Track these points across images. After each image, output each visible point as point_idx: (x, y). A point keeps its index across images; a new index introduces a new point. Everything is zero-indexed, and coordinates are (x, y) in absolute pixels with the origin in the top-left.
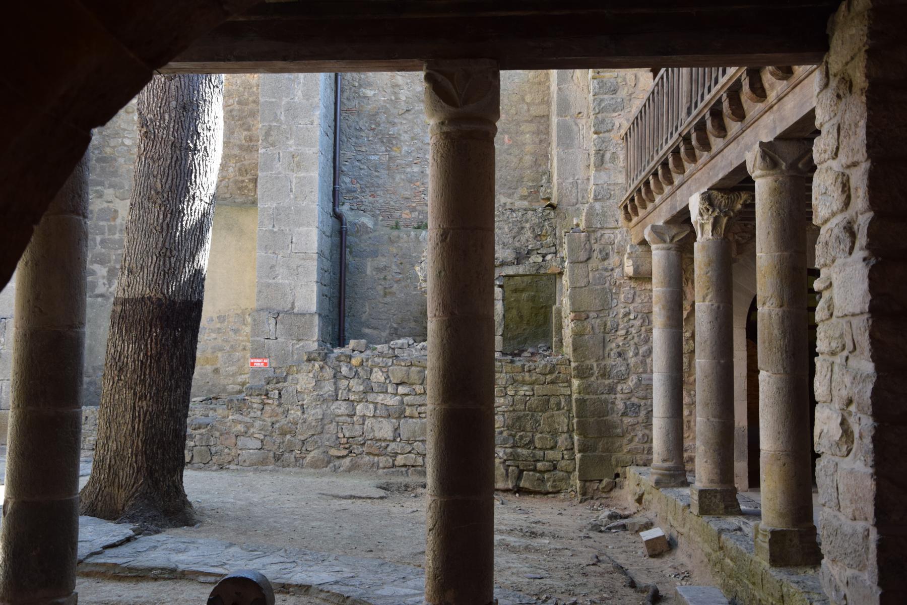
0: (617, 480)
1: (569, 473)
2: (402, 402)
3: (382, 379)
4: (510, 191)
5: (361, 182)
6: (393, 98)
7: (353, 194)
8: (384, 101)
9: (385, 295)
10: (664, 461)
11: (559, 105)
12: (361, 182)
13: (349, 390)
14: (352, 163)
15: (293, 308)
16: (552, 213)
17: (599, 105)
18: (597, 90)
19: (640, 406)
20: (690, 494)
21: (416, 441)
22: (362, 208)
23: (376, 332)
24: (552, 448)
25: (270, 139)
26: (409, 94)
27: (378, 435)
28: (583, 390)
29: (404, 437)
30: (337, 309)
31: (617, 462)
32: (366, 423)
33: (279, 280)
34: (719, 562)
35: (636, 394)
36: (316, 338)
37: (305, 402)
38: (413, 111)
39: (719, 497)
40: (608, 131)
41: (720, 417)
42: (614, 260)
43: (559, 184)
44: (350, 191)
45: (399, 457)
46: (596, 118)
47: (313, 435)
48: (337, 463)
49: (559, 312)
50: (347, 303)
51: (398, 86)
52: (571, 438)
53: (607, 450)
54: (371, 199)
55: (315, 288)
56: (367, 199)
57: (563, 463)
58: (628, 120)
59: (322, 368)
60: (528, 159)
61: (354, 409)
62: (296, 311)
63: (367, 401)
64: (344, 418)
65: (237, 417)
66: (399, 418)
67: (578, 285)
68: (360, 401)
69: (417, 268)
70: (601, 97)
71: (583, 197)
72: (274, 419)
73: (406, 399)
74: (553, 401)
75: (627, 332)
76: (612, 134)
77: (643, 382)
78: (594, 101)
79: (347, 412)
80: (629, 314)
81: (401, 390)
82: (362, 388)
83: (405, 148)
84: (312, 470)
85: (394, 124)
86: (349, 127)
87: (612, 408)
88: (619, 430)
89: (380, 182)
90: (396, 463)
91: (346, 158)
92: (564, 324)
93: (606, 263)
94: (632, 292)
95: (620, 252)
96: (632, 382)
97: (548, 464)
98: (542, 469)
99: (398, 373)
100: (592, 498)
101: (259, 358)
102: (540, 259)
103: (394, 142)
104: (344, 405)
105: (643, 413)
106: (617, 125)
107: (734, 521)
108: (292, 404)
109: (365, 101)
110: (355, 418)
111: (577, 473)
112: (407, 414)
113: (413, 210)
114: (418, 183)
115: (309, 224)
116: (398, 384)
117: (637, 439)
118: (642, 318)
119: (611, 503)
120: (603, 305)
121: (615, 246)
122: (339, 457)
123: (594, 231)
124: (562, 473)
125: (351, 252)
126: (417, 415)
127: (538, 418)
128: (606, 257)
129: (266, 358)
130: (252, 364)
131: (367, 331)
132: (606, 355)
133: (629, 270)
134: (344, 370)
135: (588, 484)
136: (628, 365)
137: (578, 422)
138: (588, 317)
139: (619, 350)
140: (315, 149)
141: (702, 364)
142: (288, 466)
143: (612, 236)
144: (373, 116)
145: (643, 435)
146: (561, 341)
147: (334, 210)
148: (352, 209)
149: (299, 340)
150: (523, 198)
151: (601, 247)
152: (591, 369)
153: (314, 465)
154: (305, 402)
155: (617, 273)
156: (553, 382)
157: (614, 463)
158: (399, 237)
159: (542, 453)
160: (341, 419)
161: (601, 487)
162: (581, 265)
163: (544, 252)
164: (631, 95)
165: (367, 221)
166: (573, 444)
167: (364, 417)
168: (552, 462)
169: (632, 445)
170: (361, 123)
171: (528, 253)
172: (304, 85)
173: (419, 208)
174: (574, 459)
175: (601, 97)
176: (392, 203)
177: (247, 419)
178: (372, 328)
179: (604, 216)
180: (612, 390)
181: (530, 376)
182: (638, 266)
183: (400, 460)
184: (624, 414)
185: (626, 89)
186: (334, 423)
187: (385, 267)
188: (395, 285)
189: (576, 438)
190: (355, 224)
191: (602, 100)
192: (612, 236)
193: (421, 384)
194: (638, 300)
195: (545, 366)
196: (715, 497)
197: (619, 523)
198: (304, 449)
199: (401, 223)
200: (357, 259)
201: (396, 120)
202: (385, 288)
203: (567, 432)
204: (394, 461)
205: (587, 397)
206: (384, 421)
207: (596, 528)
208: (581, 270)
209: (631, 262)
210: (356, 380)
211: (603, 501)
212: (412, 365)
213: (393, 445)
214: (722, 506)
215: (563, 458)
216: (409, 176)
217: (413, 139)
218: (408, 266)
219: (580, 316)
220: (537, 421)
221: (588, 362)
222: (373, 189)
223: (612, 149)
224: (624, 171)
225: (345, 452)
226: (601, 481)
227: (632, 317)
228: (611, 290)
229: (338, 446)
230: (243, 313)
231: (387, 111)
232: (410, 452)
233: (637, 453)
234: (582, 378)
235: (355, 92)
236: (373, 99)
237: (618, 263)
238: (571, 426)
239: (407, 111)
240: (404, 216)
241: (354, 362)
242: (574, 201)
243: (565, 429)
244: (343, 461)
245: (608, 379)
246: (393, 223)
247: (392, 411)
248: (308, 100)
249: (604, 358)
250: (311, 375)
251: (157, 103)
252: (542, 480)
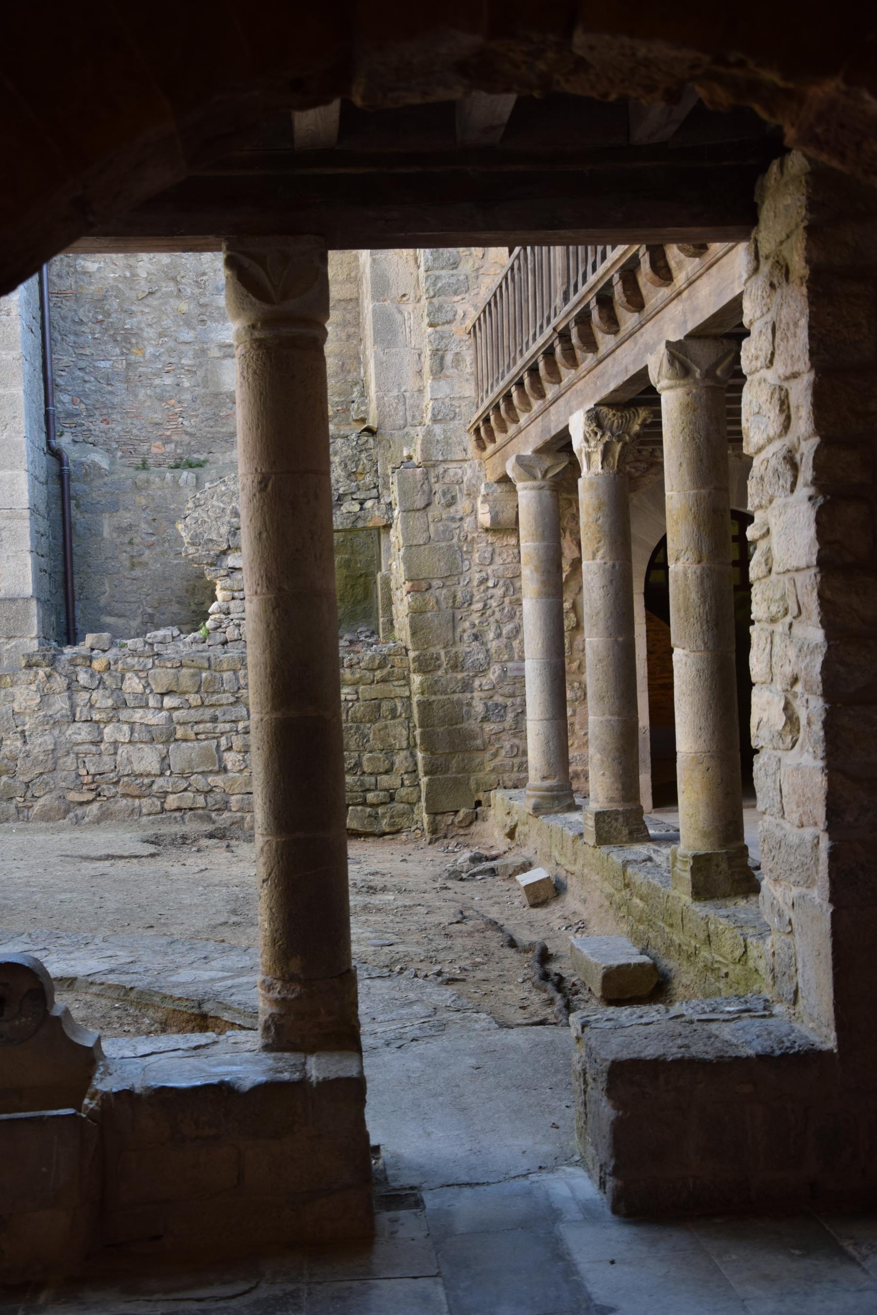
0: (479, 809)
1: (412, 804)
2: (170, 719)
3: (140, 688)
5: (87, 402)
6: (128, 274)
7: (75, 420)
8: (115, 279)
9: (133, 566)
10: (544, 778)
11: (374, 284)
12: (87, 402)
13: (92, 706)
14: (71, 373)
16: (371, 440)
17: (434, 284)
18: (430, 263)
19: (506, 707)
20: (583, 821)
21: (193, 774)
22: (90, 440)
23: (121, 622)
24: (387, 772)
26: (153, 268)
27: (138, 768)
28: (429, 688)
29: (176, 769)
30: (62, 591)
31: (478, 784)
32: (120, 751)
34: (626, 903)
35: (500, 691)
36: (34, 633)
37: (26, 727)
38: (158, 294)
39: (621, 820)
40: (449, 322)
41: (619, 715)
42: (463, 505)
43: (379, 399)
44: (70, 415)
45: (171, 797)
46: (430, 303)
47: (41, 774)
48: (79, 811)
49: (387, 582)
50: (76, 581)
52: (413, 756)
53: (464, 770)
54: (103, 426)
55: (29, 560)
56: (98, 427)
57: (403, 792)
58: (475, 307)
59: (49, 676)
61: (101, 733)
63: (119, 721)
64: (86, 746)
66: (167, 742)
67: (415, 543)
68: (109, 721)
69: (180, 526)
70: (437, 273)
71: (414, 417)
73: (176, 714)
74: (385, 706)
75: (485, 605)
76: (453, 327)
77: (509, 674)
78: (427, 278)
79: (90, 738)
80: (487, 580)
81: (168, 702)
82: (110, 702)
83: (150, 350)
84: (44, 824)
85: (131, 314)
86: (64, 318)
87: (468, 712)
88: (479, 742)
89: (116, 400)
90: (166, 806)
91: (62, 364)
92: (394, 599)
93: (452, 510)
94: (490, 549)
95: (471, 494)
96: (494, 673)
97: (382, 794)
98: (375, 801)
99: (162, 678)
100: (445, 837)
102: (357, 507)
103: (134, 341)
104: (85, 727)
105: (510, 716)
106: (460, 313)
107: (642, 850)
108: (7, 730)
109: (86, 279)
110: (103, 746)
111: (423, 804)
112: (178, 736)
113: (167, 440)
114: (173, 402)
115: (13, 466)
116: (163, 695)
117: (503, 753)
118: (504, 585)
119: (471, 842)
120: (450, 569)
121: (464, 486)
122: (81, 804)
123: (434, 466)
124: (402, 805)
125: (78, 506)
126: (193, 737)
127: (366, 731)
128: (452, 502)
131: (109, 620)
132: (457, 639)
133: (485, 518)
134: (83, 678)
135: (439, 818)
136: (487, 651)
137: (423, 734)
138: (430, 587)
139: (475, 630)
140: (16, 354)
141: (593, 643)
142: (7, 820)
143: (459, 471)
144: (100, 301)
145: (512, 747)
146: (391, 622)
147: (48, 444)
148: (75, 442)
151: (445, 487)
152: (437, 659)
153: (46, 816)
154: (26, 727)
155: (467, 524)
156: (384, 680)
157: (473, 786)
158: (148, 481)
159: (373, 779)
160: (82, 748)
161: (457, 820)
162: (417, 514)
163: (362, 497)
164: (477, 270)
165: (99, 458)
166: (416, 764)
167: (115, 744)
168: (387, 790)
169: (497, 761)
170: (81, 312)
171: (339, 499)
173: (175, 438)
174: (418, 785)
175: (437, 273)
176: (135, 431)
178: (116, 615)
179: (447, 444)
180: (467, 687)
181: (353, 673)
182: (497, 513)
183: (172, 801)
184: (485, 719)
185: (471, 262)
186: (72, 756)
187: (130, 526)
188: (147, 552)
189: (420, 755)
190: (82, 464)
191: (438, 278)
192: (460, 471)
193: (197, 692)
194: (498, 560)
195: (373, 658)
196: (616, 820)
197: (486, 867)
198: (29, 794)
199: (151, 461)
200: (87, 516)
201: (134, 308)
202: (132, 557)
203: (407, 748)
204: (162, 803)
205: (433, 698)
206: (146, 748)
207: (456, 875)
208: (417, 521)
209: (487, 508)
210: (101, 691)
211: (461, 839)
212: (181, 666)
213: (160, 781)
214: (625, 832)
215: (402, 785)
216: (158, 390)
217: (161, 335)
218: (165, 524)
219: (419, 585)
220: (365, 736)
221: (432, 650)
222: (105, 411)
223: (454, 348)
224: (472, 378)
225: (90, 796)
226: (457, 812)
227: (490, 584)
228: (460, 548)
229: (79, 787)
231: (119, 294)
232: (185, 790)
233: (504, 772)
234: (424, 672)
235: (69, 266)
236: (98, 275)
237: (468, 511)
238: (411, 740)
240: (154, 450)
241: (97, 665)
242: (402, 422)
243: (404, 744)
244: (87, 808)
245: (462, 671)
246: (138, 461)
247: (156, 732)
249: (454, 643)
250: (33, 687)
252: (376, 817)
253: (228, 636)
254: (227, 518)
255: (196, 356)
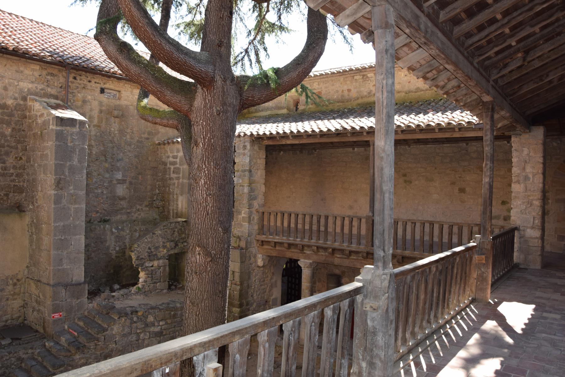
4: (141, 203)
13: (137, 328)
15: (72, 281)
25: (60, 186)
33: (65, 266)
36: (87, 295)
42: (253, 259)
51: (92, 146)
60: (149, 187)
61: (139, 336)
62: (73, 282)
65: (82, 356)
66: (160, 337)
68: (142, 332)
72: (102, 352)
73: (163, 327)
81: (161, 323)
82: (143, 326)
83: (94, 180)
95: (255, 257)
101: (57, 313)
110: (140, 341)
112: (164, 334)
113: (97, 212)
115: (80, 234)
129: (61, 312)
130: (53, 317)
134: (135, 319)
149: (78, 299)
150: (146, 206)
158: (95, 228)
167: (144, 340)
172: (79, 155)
177: (88, 356)
188: (93, 254)
217: (99, 175)
230: (7, 278)
239: (97, 160)
240: (93, 215)
248: (80, 164)
251: (218, 246)
253: (146, 290)
254: (147, 250)
255: (109, 183)
